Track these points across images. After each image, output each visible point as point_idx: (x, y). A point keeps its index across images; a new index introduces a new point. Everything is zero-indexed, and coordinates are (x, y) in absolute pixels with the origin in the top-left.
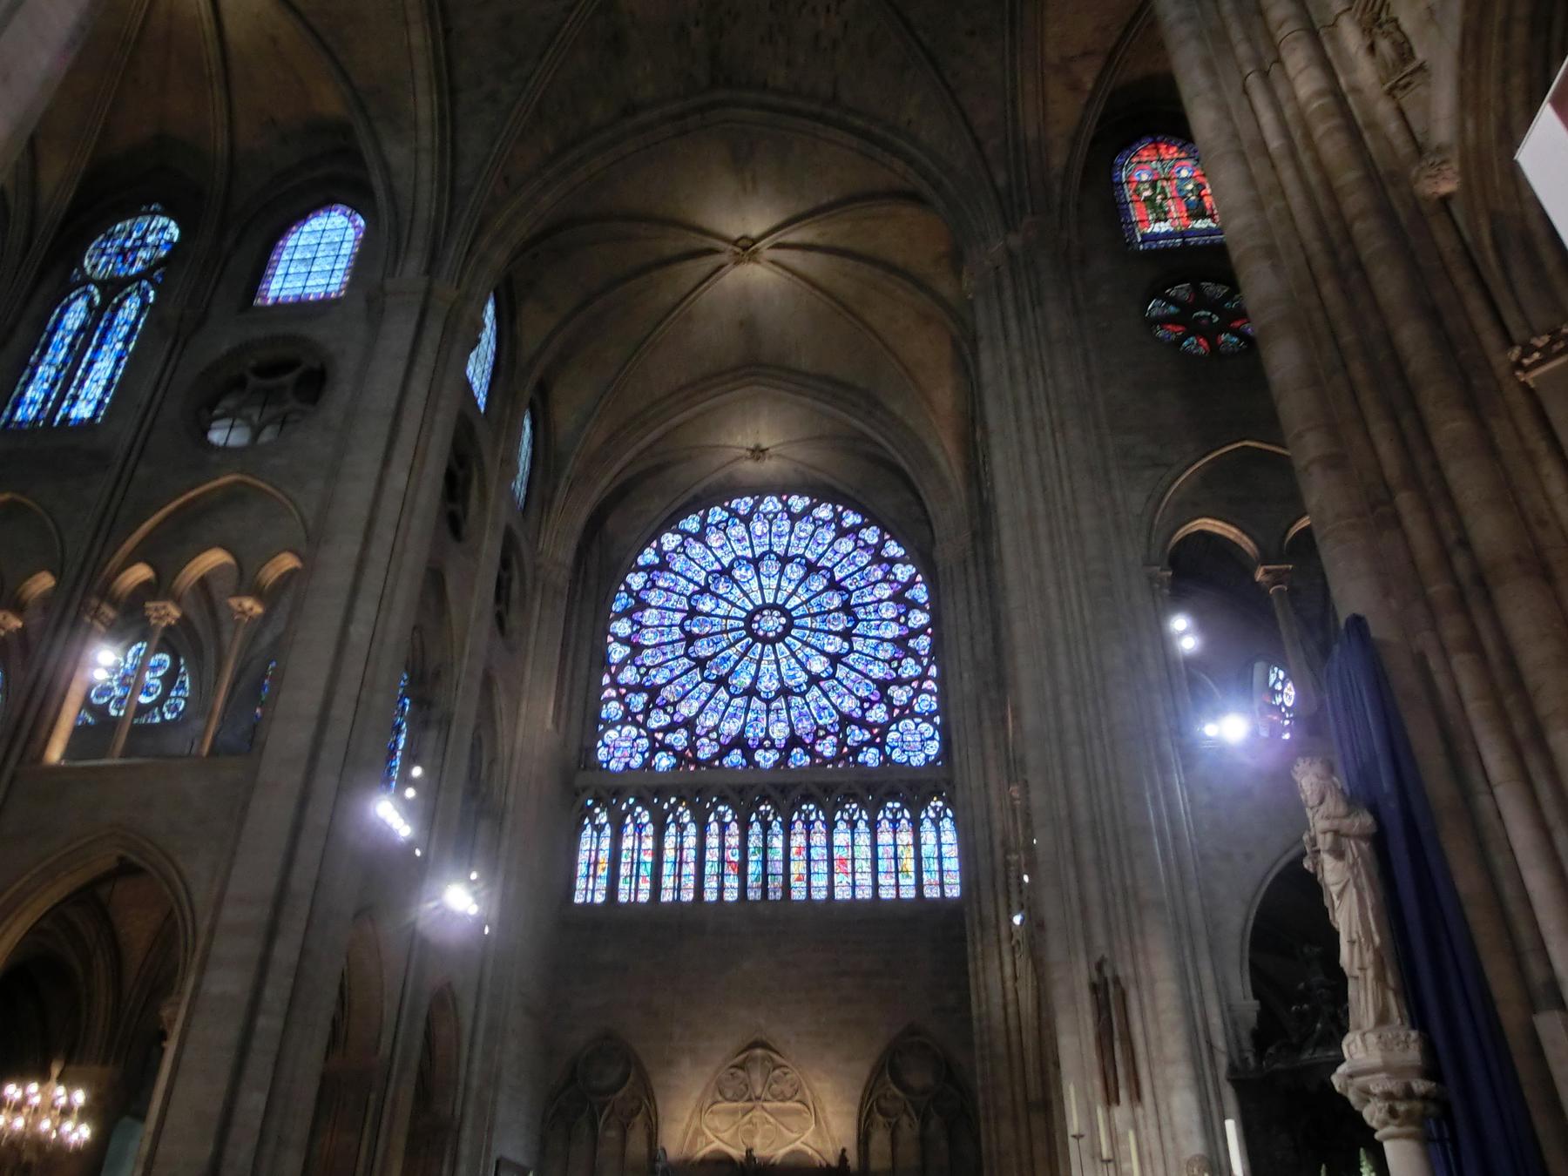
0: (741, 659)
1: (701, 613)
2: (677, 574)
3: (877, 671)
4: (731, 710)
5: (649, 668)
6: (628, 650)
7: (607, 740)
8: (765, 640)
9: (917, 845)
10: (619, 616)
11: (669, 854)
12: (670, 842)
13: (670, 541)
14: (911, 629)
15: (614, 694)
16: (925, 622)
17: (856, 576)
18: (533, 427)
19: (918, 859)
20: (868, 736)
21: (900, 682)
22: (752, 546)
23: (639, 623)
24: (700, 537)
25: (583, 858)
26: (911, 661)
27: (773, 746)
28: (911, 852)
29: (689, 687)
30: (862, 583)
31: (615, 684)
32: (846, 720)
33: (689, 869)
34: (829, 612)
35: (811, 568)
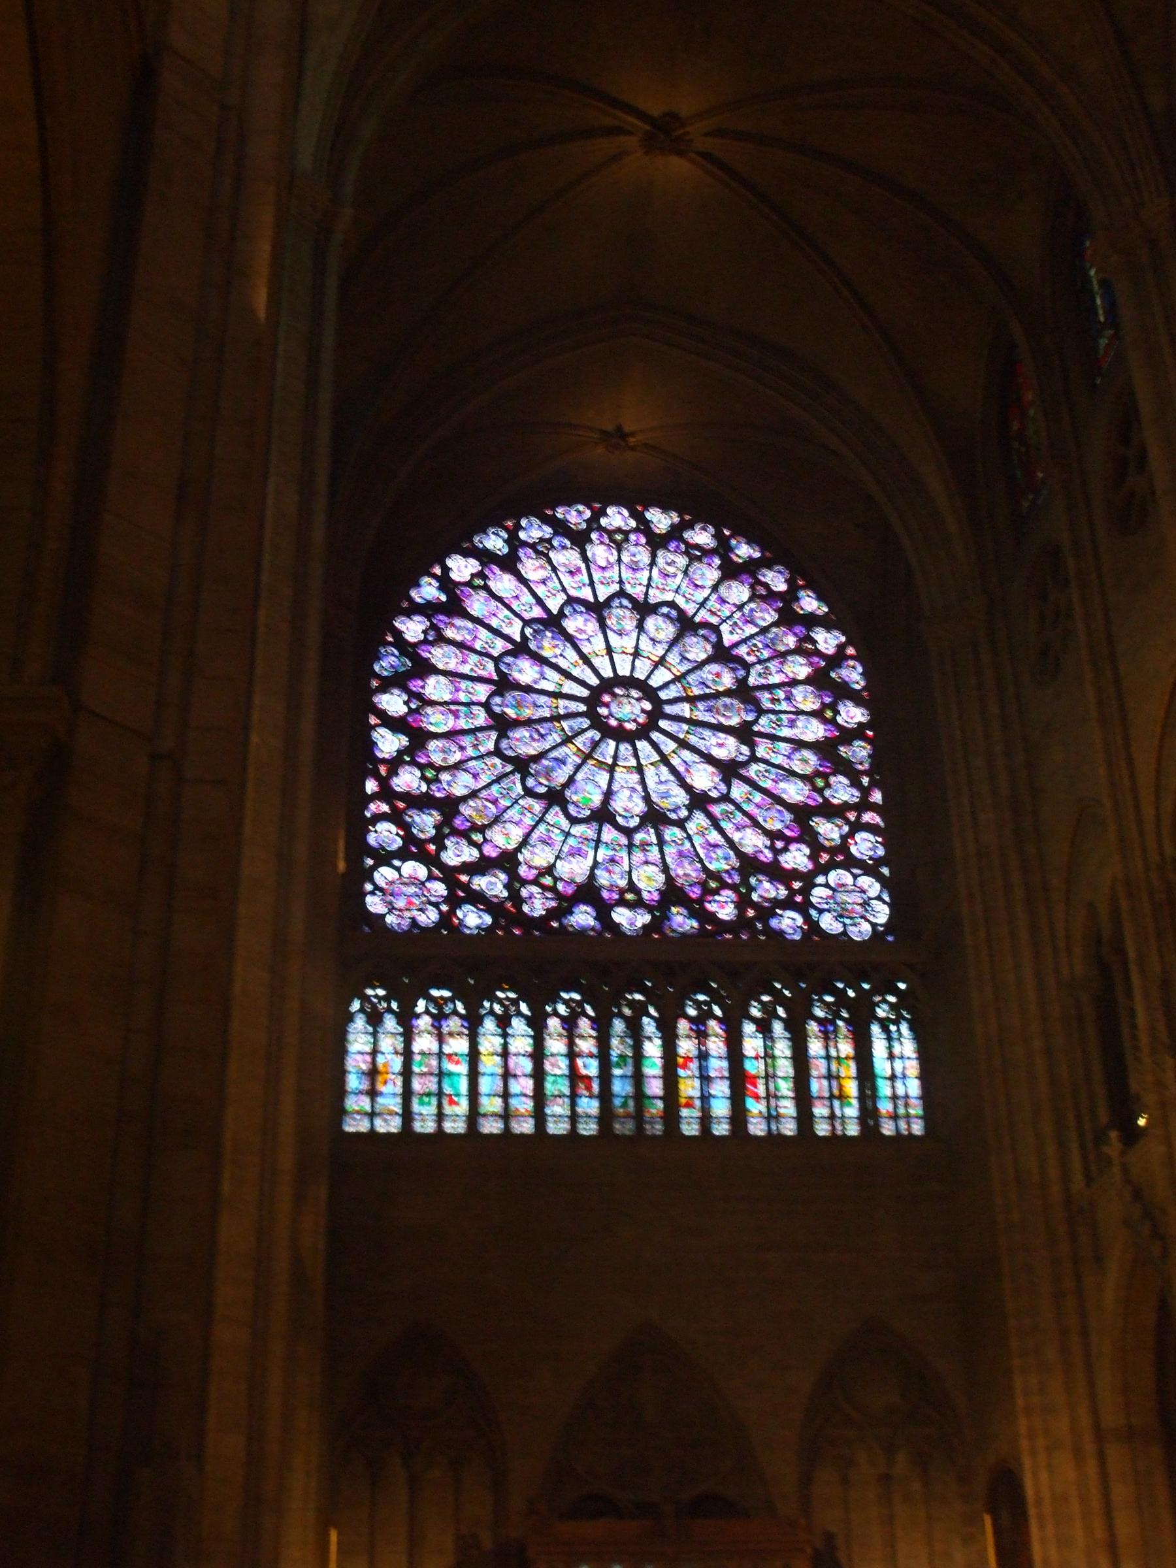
0: (584, 762)
1: (517, 686)
3: (795, 792)
4: (572, 841)
5: (439, 769)
6: (404, 741)
8: (620, 735)
10: (387, 685)
11: (490, 1064)
12: (490, 1042)
13: (461, 568)
15: (385, 808)
16: (864, 719)
20: (783, 892)
21: (830, 811)
23: (419, 697)
26: (845, 781)
27: (638, 904)
29: (505, 803)
30: (766, 654)
32: (749, 865)
34: (717, 695)
35: (686, 625)
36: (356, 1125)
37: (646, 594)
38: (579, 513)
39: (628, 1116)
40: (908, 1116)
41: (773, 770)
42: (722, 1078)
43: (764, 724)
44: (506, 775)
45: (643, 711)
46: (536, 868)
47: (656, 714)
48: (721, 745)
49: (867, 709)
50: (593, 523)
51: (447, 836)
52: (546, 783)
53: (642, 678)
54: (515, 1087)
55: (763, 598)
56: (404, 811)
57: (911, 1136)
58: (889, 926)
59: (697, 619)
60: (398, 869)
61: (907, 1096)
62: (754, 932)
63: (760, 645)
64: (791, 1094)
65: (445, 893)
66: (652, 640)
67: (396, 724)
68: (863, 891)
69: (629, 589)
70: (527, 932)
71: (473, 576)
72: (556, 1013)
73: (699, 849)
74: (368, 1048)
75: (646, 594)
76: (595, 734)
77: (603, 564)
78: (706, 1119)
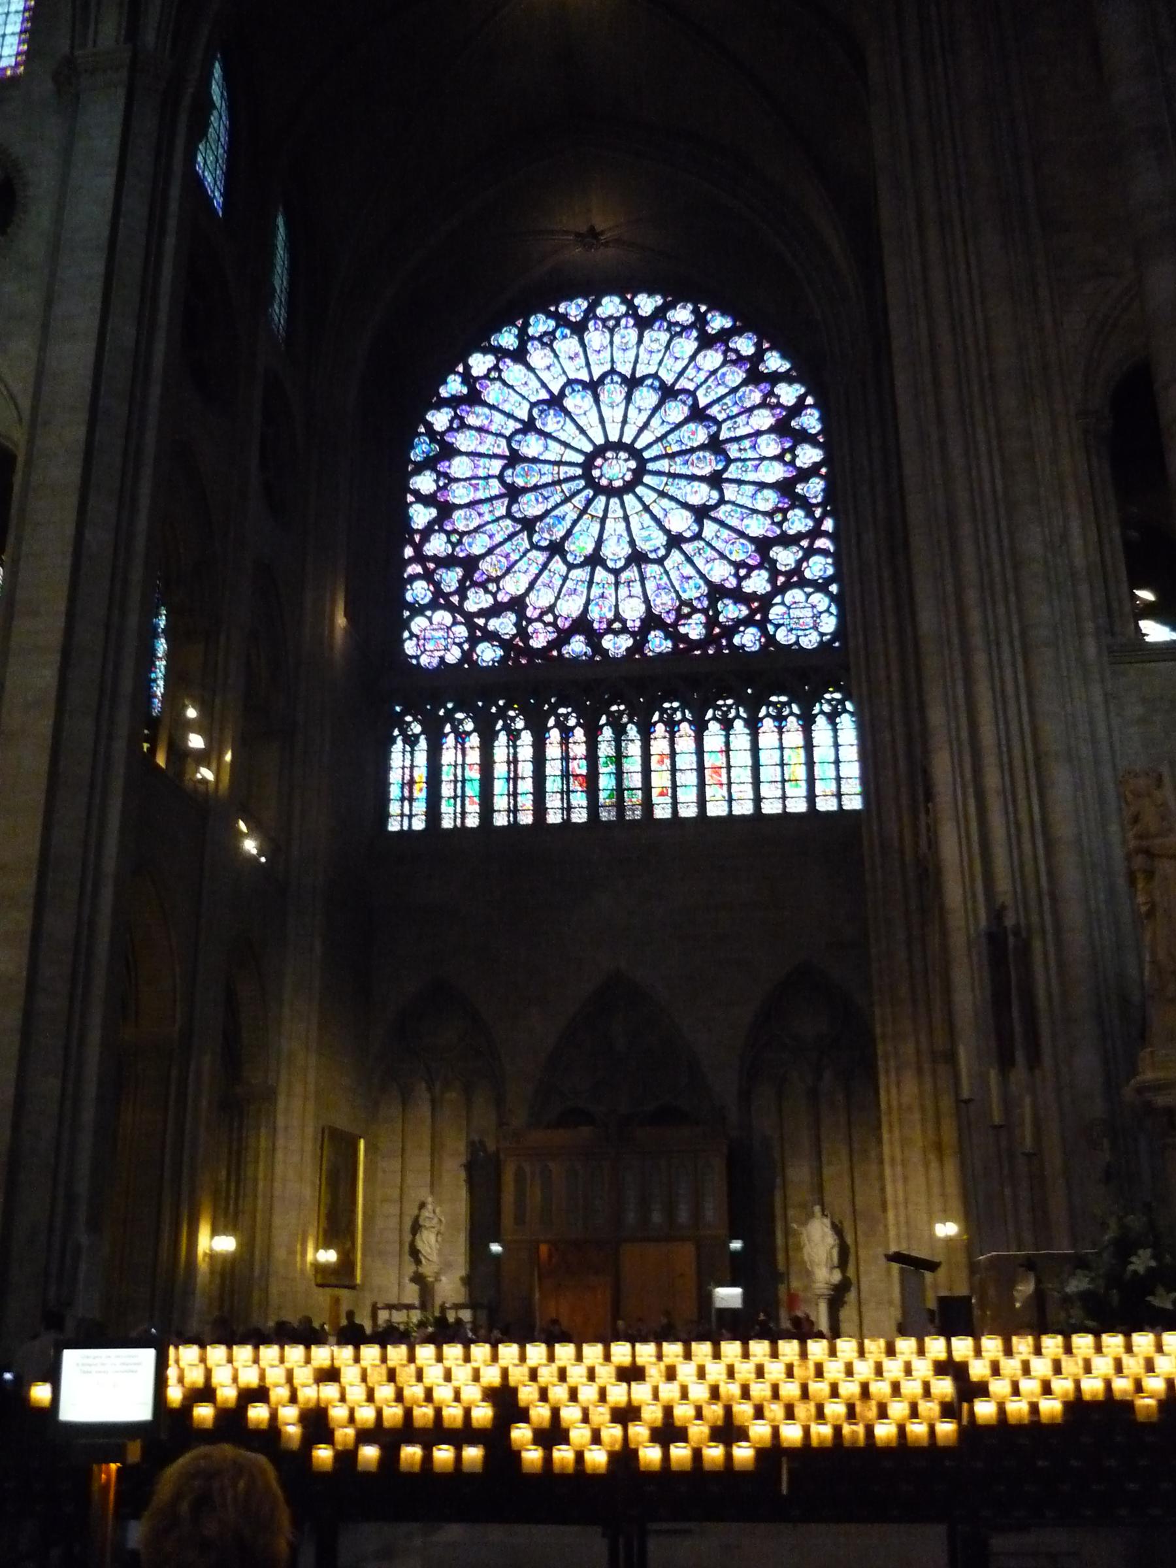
0: (580, 517)
1: (526, 459)
2: (492, 407)
3: (758, 527)
4: (569, 584)
5: (462, 534)
6: (433, 512)
8: (610, 492)
9: (809, 746)
10: (420, 468)
11: (500, 770)
12: (500, 752)
13: (480, 363)
14: (800, 469)
17: (727, 400)
18: (286, 224)
19: (810, 764)
20: (745, 612)
21: (786, 540)
22: (588, 364)
24: (519, 355)
25: (395, 777)
26: (800, 513)
27: (624, 630)
28: (801, 756)
29: (514, 557)
30: (735, 410)
31: (420, 558)
32: (716, 592)
34: (692, 450)
35: (668, 393)
36: (394, 826)
38: (579, 306)
41: (739, 510)
43: (733, 472)
45: (629, 469)
47: (640, 472)
50: (590, 314)
53: (629, 442)
56: (434, 571)
58: (836, 635)
59: (677, 387)
60: (430, 619)
62: (720, 648)
63: (730, 404)
64: (750, 780)
65: (466, 634)
68: (813, 607)
69: (620, 368)
71: (489, 370)
73: (677, 582)
76: (589, 493)
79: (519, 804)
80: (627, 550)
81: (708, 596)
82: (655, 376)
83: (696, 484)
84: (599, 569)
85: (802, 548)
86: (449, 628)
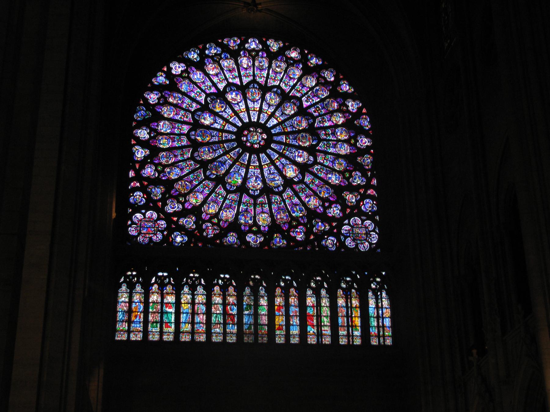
1: (203, 126)
3: (334, 179)
4: (227, 202)
5: (165, 166)
7: (136, 220)
8: (252, 150)
10: (140, 125)
11: (186, 307)
12: (186, 298)
13: (177, 68)
14: (359, 149)
15: (138, 184)
20: (328, 227)
21: (352, 189)
22: (240, 76)
23: (156, 130)
24: (200, 66)
25: (122, 307)
26: (359, 174)
27: (258, 232)
30: (323, 111)
32: (312, 214)
33: (201, 318)
34: (299, 132)
35: (285, 97)
36: (121, 337)
37: (266, 82)
38: (235, 42)
39: (250, 334)
40: (384, 336)
42: (296, 316)
44: (197, 169)
45: (263, 139)
46: (209, 214)
48: (301, 156)
49: (371, 138)
50: (241, 46)
51: (168, 198)
52: (215, 173)
53: (263, 122)
54: (197, 319)
55: (323, 85)
56: (147, 186)
57: (385, 346)
60: (144, 214)
61: (383, 326)
62: (313, 247)
64: (329, 324)
66: (267, 104)
67: (144, 144)
68: (366, 228)
69: (258, 79)
70: (204, 245)
71: (182, 72)
72: (218, 284)
74: (127, 300)
75: (266, 82)
77: (245, 66)
78: (288, 336)
79: (196, 329)
80: (260, 185)
81: (307, 216)
82: (279, 87)
83: (301, 151)
84: (244, 195)
85: (360, 193)
86: (156, 221)
